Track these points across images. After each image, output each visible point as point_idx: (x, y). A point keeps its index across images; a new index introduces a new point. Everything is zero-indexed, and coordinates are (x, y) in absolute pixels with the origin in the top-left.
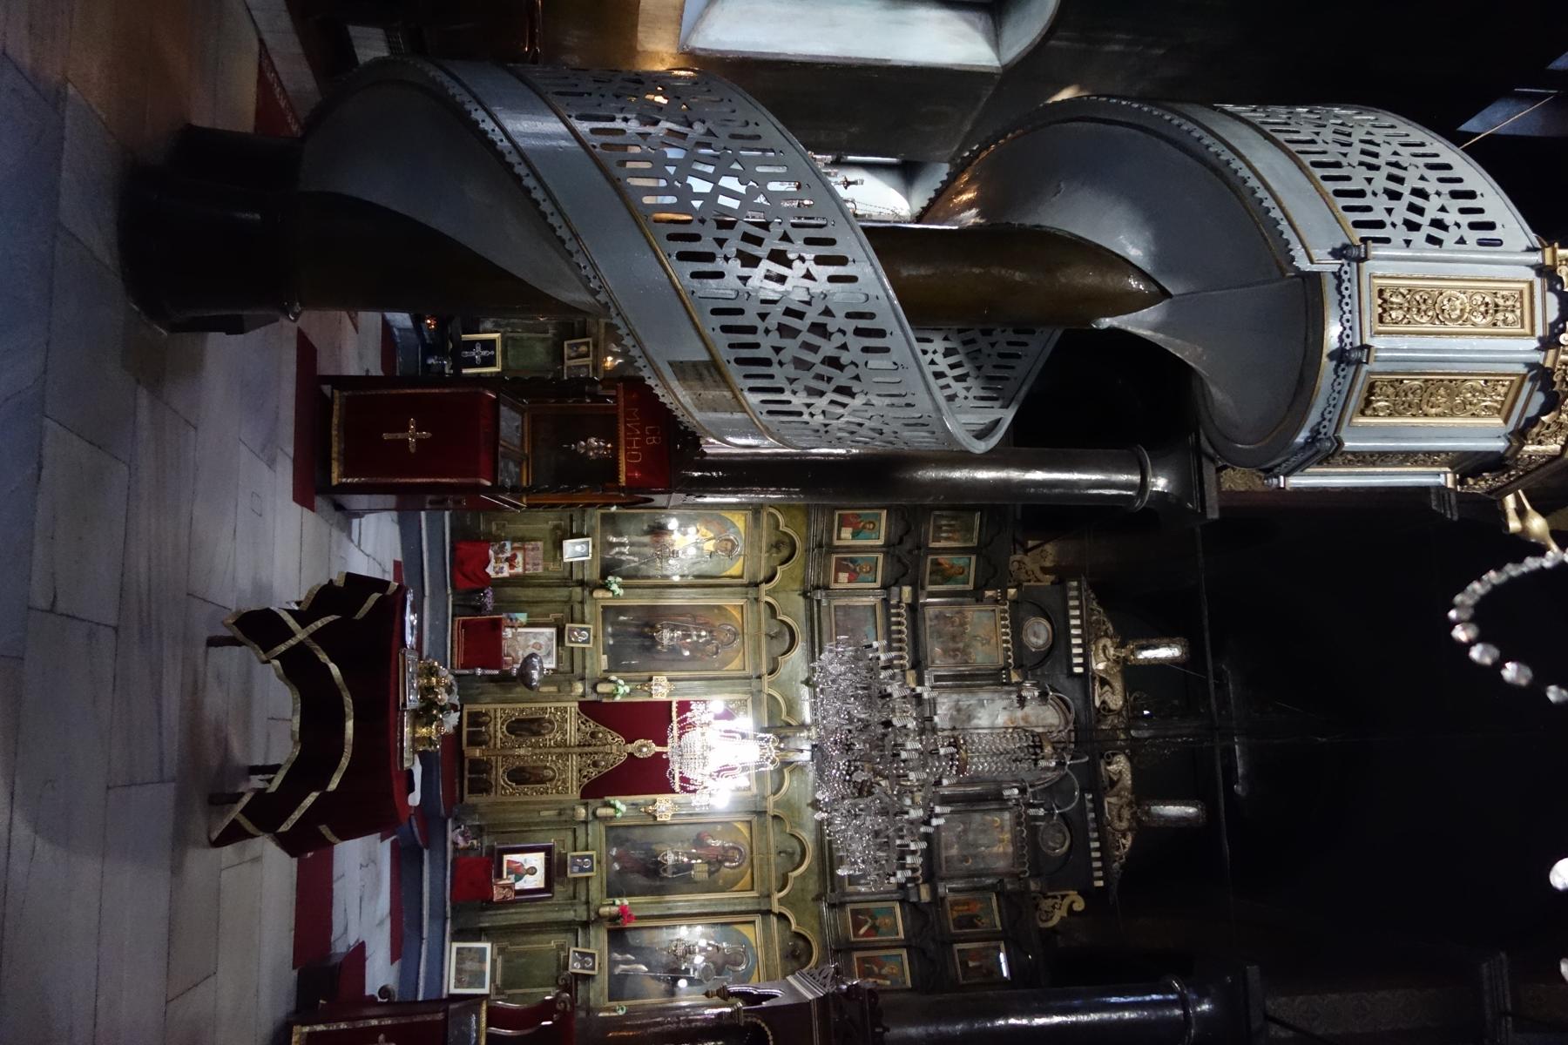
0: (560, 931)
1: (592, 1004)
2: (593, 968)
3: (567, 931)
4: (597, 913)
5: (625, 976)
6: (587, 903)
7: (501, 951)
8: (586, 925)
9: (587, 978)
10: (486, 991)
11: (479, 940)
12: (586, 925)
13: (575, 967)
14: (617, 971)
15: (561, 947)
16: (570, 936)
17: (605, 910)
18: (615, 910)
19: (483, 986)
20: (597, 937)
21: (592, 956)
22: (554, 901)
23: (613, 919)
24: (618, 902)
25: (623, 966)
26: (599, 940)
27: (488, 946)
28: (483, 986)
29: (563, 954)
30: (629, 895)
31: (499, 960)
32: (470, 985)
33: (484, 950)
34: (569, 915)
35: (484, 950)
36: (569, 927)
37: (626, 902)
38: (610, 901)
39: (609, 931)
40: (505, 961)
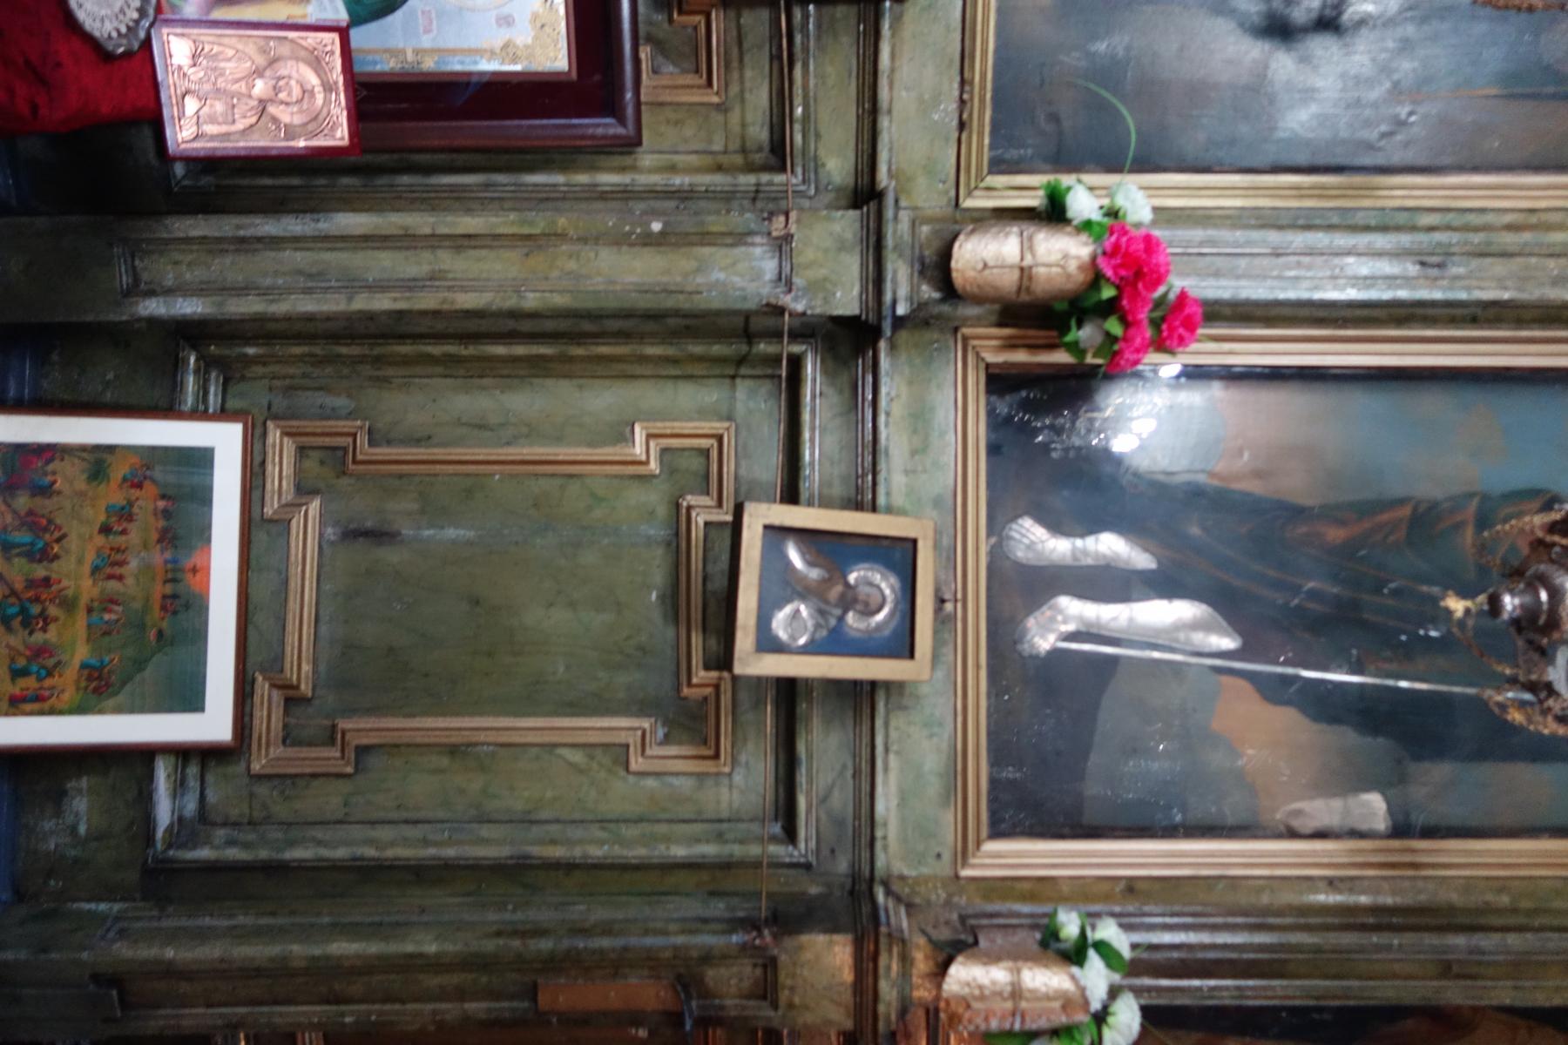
0: (680, 370)
1: (891, 857)
2: (902, 644)
3: (734, 368)
4: (938, 268)
5: (1082, 678)
6: (865, 195)
7: (328, 465)
8: (853, 340)
9: (860, 699)
10: (213, 723)
11: (167, 409)
12: (853, 340)
13: (780, 637)
14: (1043, 637)
15: (699, 469)
16: (756, 405)
17: (988, 255)
18: (1060, 256)
19: (190, 699)
20: (919, 418)
21: (899, 555)
22: (647, 169)
23: (1034, 313)
24: (1083, 202)
25: (1074, 610)
26: (933, 421)
27: (224, 441)
28: (190, 699)
29: (704, 512)
30: (1144, 165)
31: (308, 530)
32: (99, 691)
33: (201, 459)
34: (741, 274)
35: (201, 459)
36: (746, 341)
37: (1138, 199)
38: (1027, 189)
39: (999, 381)
40: (355, 534)
